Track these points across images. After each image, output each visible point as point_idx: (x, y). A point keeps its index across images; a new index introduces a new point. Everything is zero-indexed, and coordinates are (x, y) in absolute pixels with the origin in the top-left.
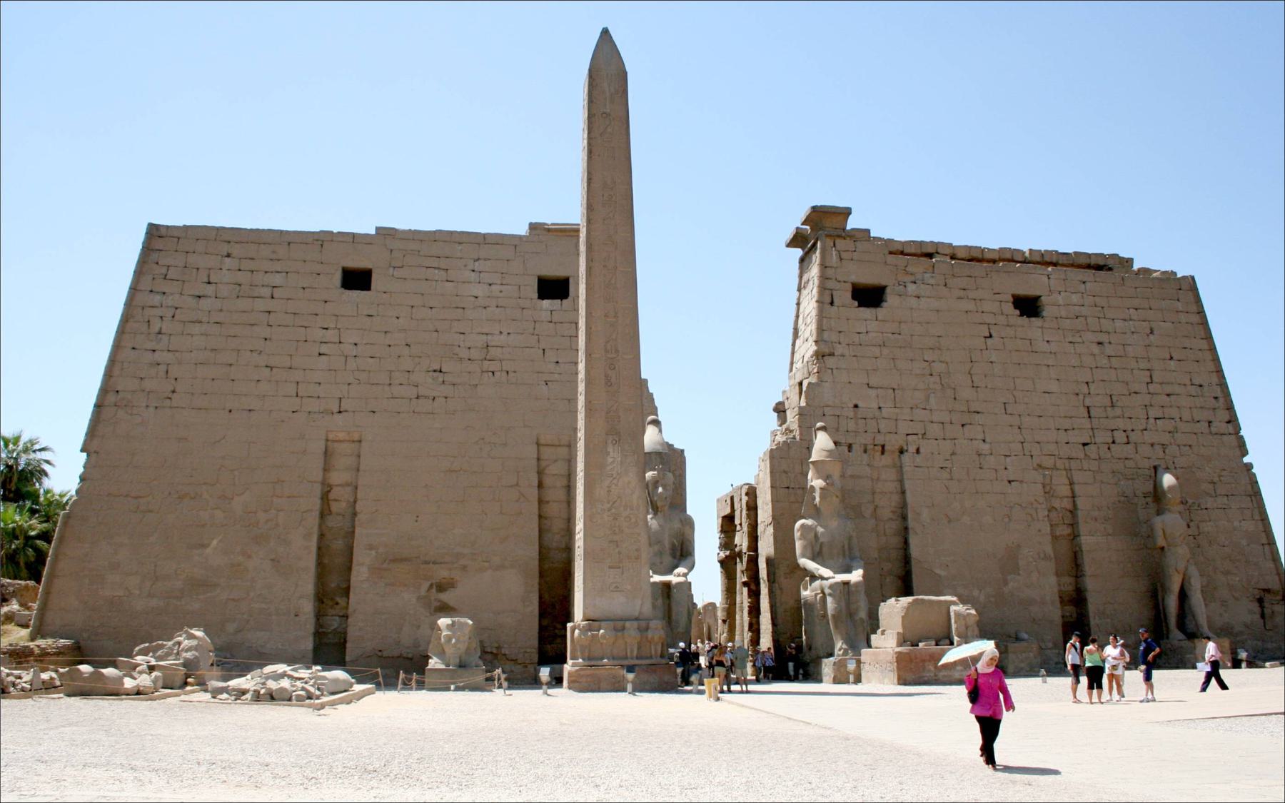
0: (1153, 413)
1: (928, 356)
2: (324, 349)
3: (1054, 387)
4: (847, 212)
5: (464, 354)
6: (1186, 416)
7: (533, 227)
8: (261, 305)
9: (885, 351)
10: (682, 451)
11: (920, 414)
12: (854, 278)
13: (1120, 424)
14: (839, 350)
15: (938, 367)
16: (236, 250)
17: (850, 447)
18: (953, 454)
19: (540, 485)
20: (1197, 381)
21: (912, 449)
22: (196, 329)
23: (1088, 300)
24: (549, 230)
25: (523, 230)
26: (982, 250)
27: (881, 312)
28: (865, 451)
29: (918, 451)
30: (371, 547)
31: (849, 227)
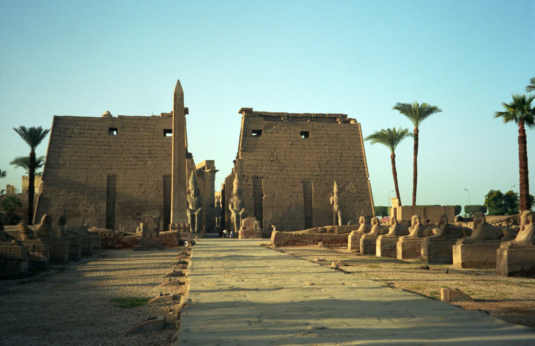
0: (340, 166)
1: (273, 151)
2: (106, 151)
3: (311, 159)
4: (252, 109)
5: (143, 152)
6: (351, 166)
8: (87, 138)
9: (260, 150)
11: (269, 167)
13: (329, 169)
16: (79, 123)
20: (356, 156)
22: (70, 146)
23: (324, 132)
26: (297, 114)
27: (260, 138)
30: (119, 204)
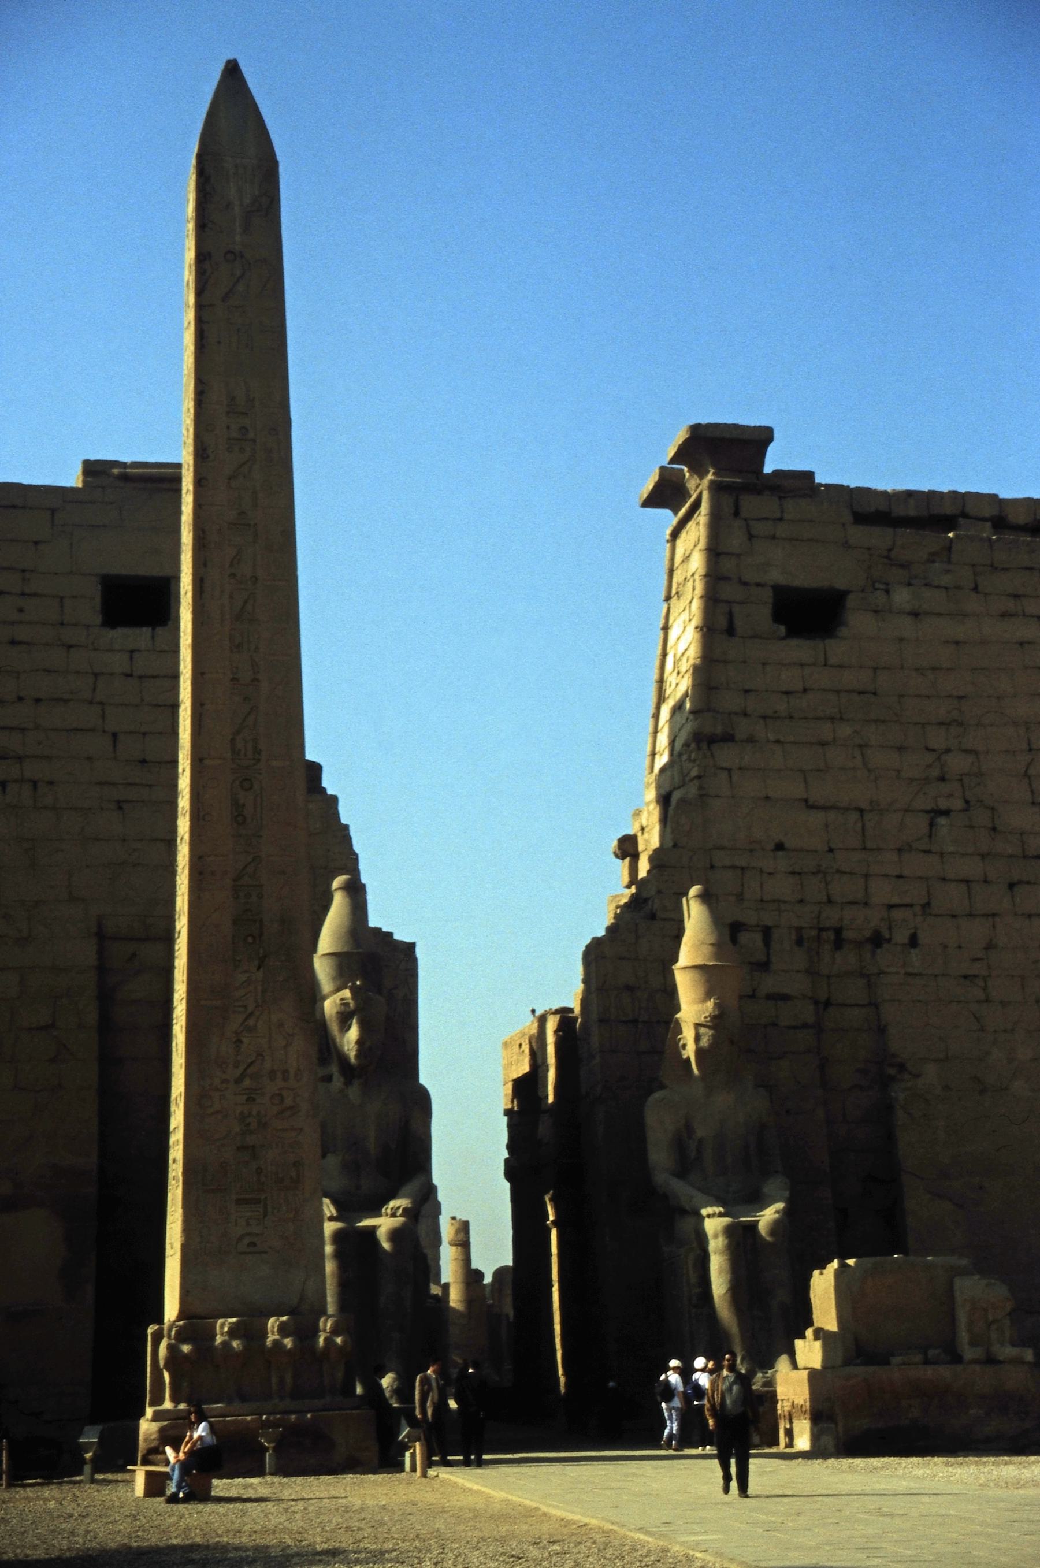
1: (938, 739)
4: (762, 438)
7: (93, 469)
9: (845, 730)
10: (412, 946)
12: (775, 576)
14: (743, 728)
15: (957, 763)
17: (767, 932)
18: (990, 946)
19: (106, 1025)
21: (901, 936)
24: (125, 478)
25: (72, 478)
27: (837, 649)
28: (799, 942)
29: (913, 941)
31: (768, 469)
